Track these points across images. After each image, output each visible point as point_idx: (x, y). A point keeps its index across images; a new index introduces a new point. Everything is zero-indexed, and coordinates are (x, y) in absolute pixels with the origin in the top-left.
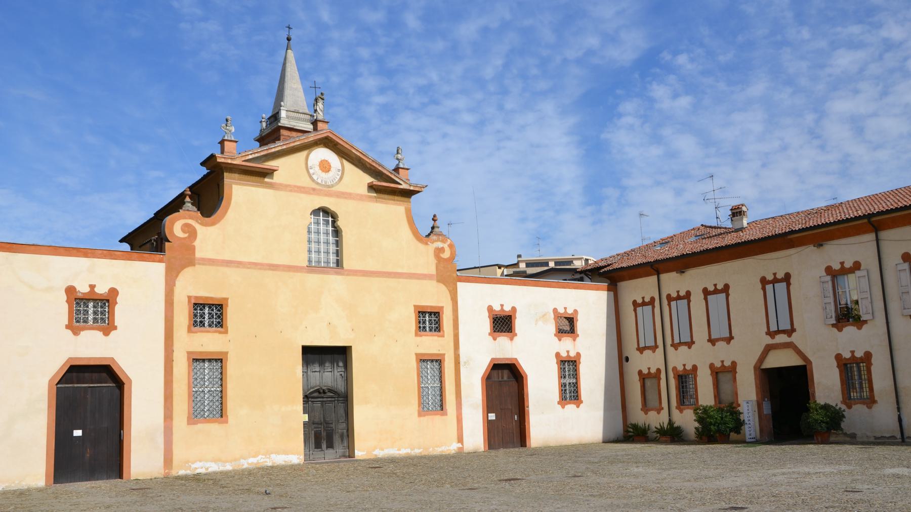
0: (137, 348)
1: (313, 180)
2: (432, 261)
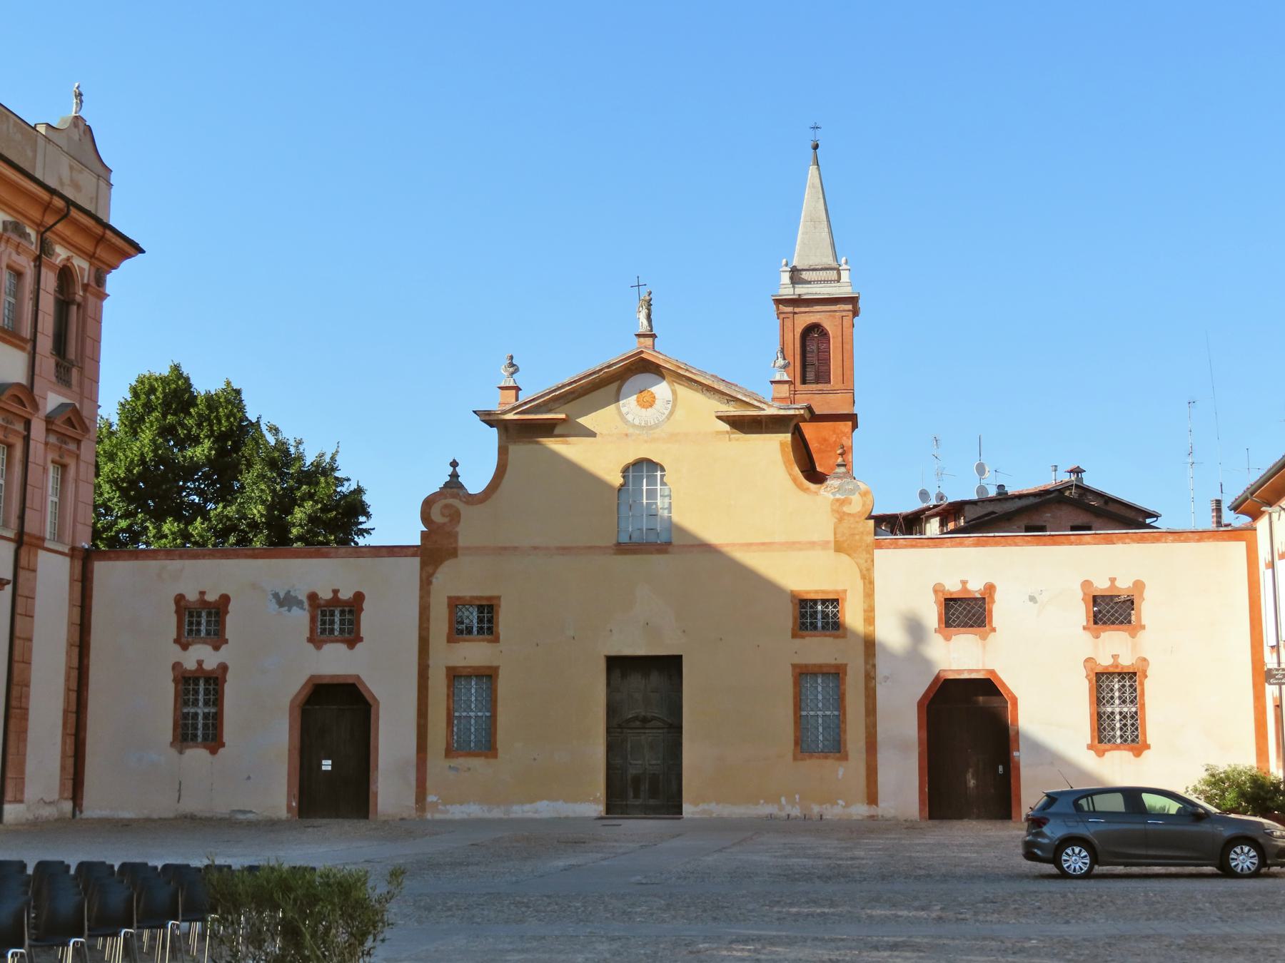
0: (383, 664)
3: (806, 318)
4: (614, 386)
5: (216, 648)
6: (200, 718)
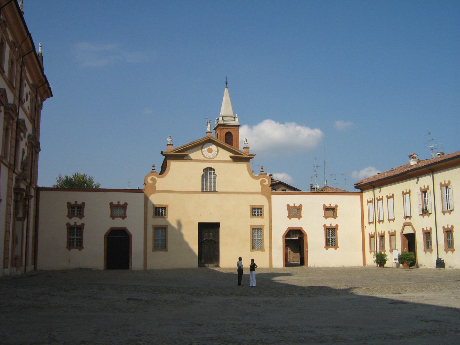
1: (205, 157)
2: (259, 186)
3: (226, 131)
4: (200, 147)
5: (81, 219)
6: (75, 240)
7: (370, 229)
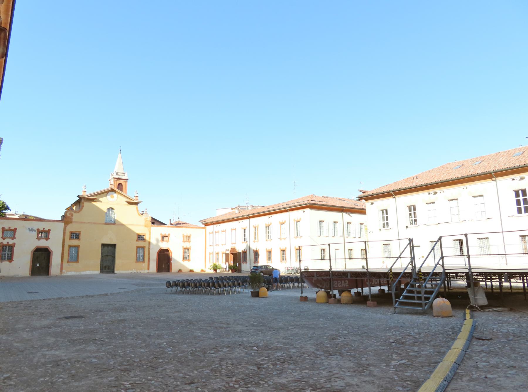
0: (55, 245)
5: (13, 239)
7: (210, 250)
